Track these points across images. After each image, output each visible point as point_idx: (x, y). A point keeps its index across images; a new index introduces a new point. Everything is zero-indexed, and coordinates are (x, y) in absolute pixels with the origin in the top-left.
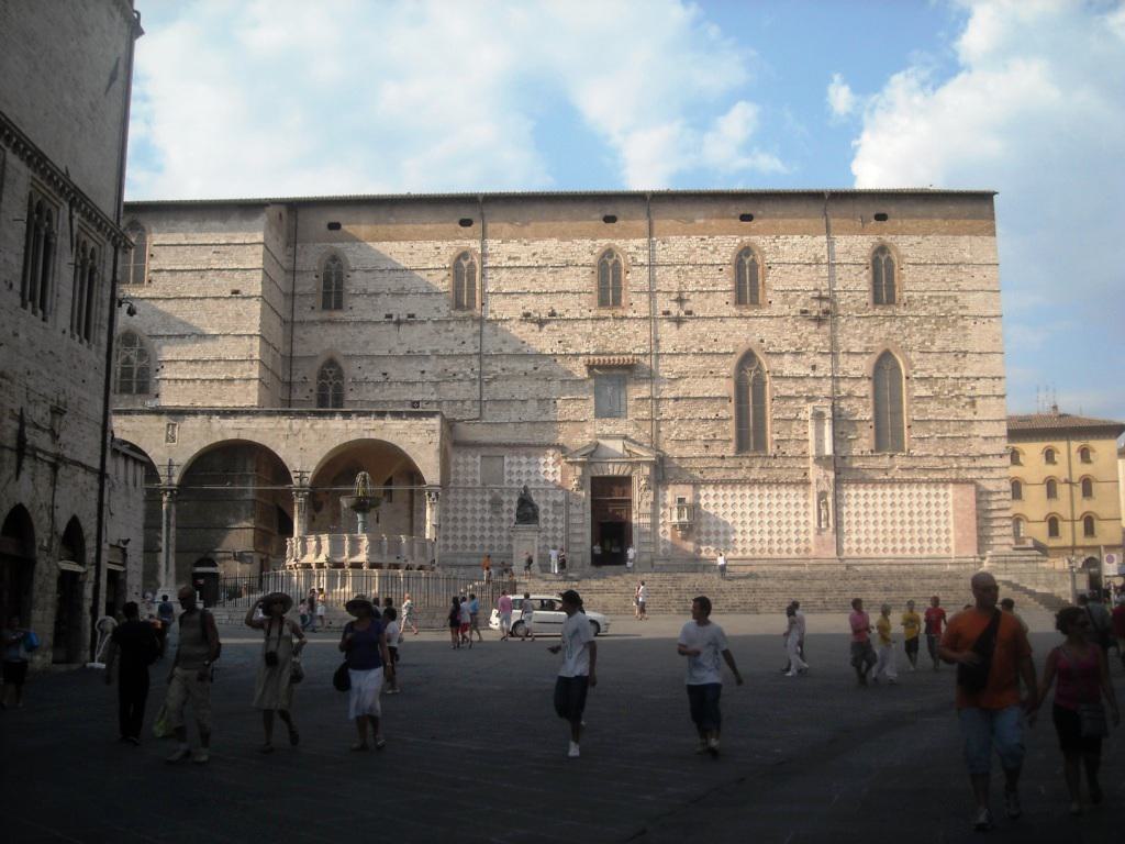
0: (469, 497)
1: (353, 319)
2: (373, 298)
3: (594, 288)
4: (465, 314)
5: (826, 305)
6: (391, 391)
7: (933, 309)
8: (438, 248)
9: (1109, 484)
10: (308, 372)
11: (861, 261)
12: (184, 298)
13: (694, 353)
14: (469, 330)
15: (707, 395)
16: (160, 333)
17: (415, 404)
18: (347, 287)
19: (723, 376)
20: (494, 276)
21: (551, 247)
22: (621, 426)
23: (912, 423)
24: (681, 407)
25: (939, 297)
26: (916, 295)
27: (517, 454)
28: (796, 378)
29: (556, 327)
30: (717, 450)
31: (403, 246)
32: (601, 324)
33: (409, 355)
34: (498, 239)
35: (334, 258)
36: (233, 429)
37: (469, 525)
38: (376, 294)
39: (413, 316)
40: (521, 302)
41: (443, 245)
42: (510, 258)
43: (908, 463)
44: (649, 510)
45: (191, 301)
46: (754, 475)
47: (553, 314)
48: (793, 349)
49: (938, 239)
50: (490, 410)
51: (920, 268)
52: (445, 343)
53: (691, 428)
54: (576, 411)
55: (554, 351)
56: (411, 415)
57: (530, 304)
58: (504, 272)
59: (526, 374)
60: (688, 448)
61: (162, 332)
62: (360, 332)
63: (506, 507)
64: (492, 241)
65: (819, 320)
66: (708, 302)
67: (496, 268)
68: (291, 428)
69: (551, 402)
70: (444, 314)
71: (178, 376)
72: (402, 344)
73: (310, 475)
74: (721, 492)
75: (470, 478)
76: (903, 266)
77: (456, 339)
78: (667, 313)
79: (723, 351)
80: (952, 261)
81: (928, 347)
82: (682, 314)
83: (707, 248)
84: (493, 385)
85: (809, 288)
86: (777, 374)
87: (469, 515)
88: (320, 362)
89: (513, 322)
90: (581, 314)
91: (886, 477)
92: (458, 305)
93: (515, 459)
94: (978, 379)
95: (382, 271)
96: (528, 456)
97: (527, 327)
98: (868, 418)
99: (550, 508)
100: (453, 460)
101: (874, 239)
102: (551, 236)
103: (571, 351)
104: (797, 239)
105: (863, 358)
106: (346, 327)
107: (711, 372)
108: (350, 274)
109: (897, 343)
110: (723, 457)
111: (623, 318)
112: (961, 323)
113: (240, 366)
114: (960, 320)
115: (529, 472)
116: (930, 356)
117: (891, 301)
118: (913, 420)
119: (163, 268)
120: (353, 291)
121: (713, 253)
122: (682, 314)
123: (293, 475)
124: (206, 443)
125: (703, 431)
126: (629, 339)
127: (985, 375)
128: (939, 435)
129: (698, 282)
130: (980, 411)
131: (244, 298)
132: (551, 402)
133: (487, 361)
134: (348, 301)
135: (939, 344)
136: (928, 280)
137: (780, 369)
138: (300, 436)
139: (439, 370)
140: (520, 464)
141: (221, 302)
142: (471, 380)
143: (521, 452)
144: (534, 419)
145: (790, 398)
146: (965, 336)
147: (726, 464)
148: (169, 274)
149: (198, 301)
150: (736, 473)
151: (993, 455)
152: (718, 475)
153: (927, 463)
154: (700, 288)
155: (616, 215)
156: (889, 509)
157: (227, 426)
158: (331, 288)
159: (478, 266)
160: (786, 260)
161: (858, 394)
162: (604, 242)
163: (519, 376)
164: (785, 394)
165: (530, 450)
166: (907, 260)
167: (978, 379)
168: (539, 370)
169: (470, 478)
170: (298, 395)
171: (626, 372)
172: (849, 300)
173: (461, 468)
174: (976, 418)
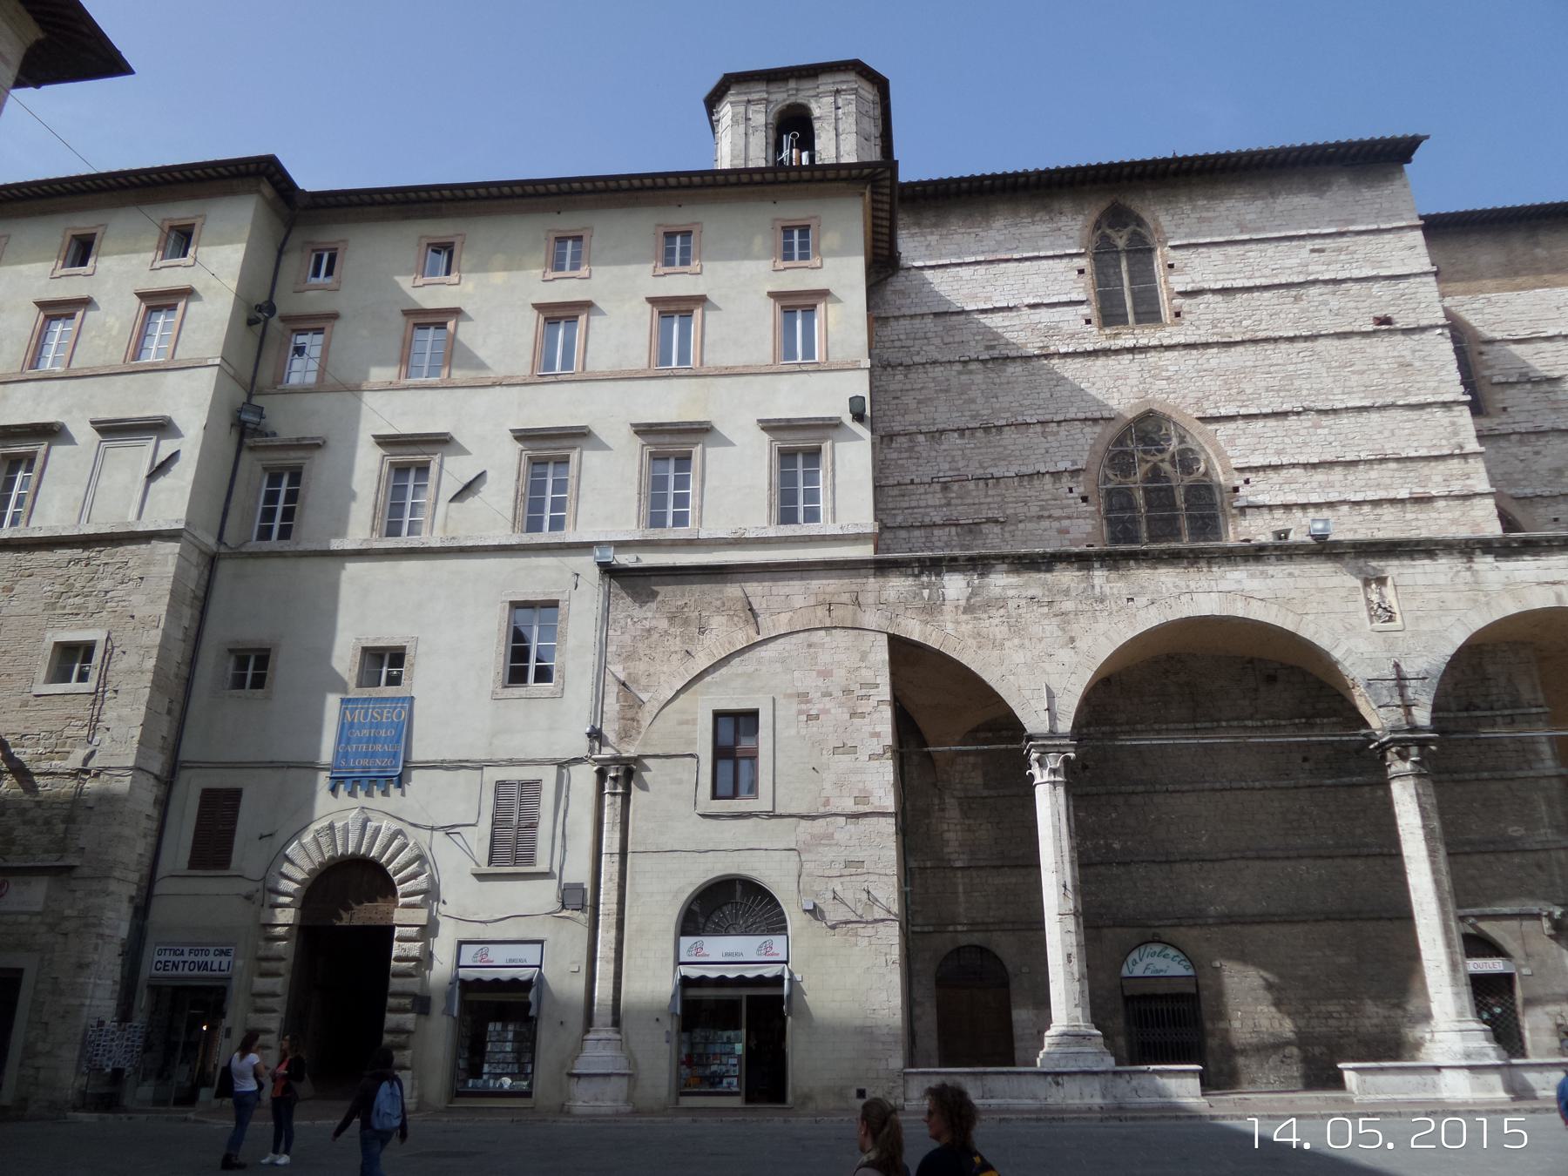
2: (1545, 387)
12: (1267, 340)
16: (1223, 412)
18: (1487, 373)
36: (1539, 584)
45: (1284, 346)
61: (1230, 410)
62: (1537, 453)
71: (1291, 498)
106: (1503, 443)
108: (1484, 348)
113: (1441, 466)
119: (1206, 286)
124: (1479, 620)
131: (1407, 332)
141: (1355, 342)
148: (1219, 298)
149: (1301, 345)
157: (1519, 576)
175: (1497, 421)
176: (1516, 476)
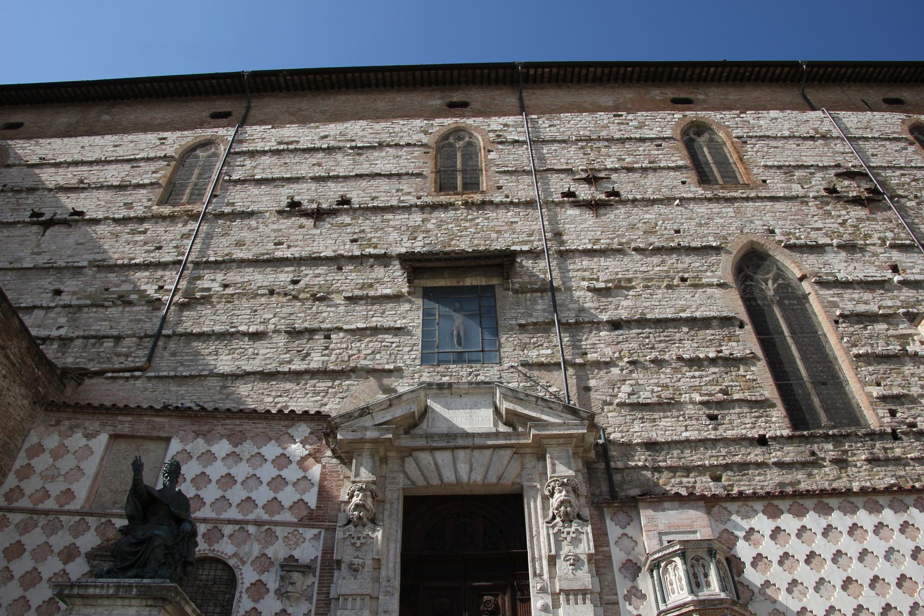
3: (428, 170)
19: (710, 285)
20: (248, 162)
24: (631, 340)
27: (205, 435)
44: (585, 578)
47: (344, 201)
50: (174, 354)
53: (664, 379)
57: (306, 194)
69: (319, 337)
72: (39, 254)
78: (570, 194)
83: (628, 124)
89: (267, 214)
90: (402, 201)
93: (200, 445)
96: (236, 439)
99: (272, 580)
100: (33, 439)
107: (683, 280)
110: (762, 441)
115: (228, 480)
121: (636, 128)
126: (499, 232)
140: (208, 457)
143: (220, 429)
144: (272, 367)
155: (467, 100)
162: (449, 122)
163: (255, 296)
165: (248, 426)
168: (302, 284)
171: (495, 281)
173: (42, 463)
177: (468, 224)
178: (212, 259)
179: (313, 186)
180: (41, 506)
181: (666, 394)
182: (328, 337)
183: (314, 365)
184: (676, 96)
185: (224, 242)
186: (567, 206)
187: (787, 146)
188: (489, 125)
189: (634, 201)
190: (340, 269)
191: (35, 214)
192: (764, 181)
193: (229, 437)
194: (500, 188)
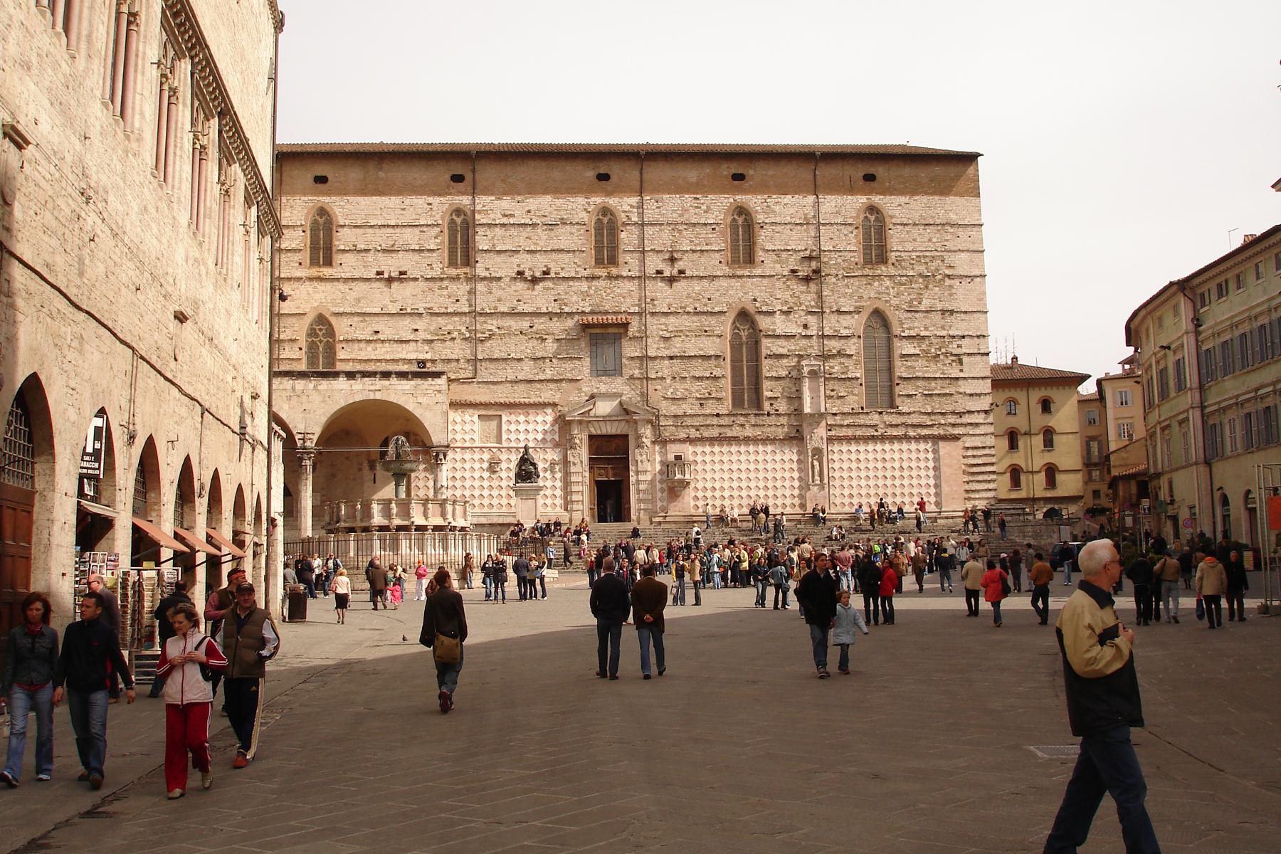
0: (468, 456)
1: (343, 275)
4: (458, 271)
5: (814, 265)
6: (384, 350)
7: (922, 269)
8: (431, 204)
9: (1070, 436)
10: (297, 331)
11: (850, 221)
13: (688, 313)
14: (462, 289)
15: (701, 353)
17: (422, 363)
18: (337, 243)
21: (544, 204)
22: (617, 384)
23: (897, 381)
25: (925, 257)
26: (903, 254)
28: (788, 337)
29: (551, 285)
30: (710, 408)
31: (394, 201)
32: (595, 283)
33: (402, 314)
34: (492, 194)
35: (322, 212)
37: (468, 483)
38: (367, 251)
39: (401, 273)
40: (516, 259)
41: (436, 200)
42: (505, 216)
43: (899, 420)
46: (749, 432)
48: (785, 308)
49: (925, 199)
51: (907, 228)
52: (440, 299)
54: (573, 369)
55: (550, 309)
56: (416, 375)
58: (497, 229)
59: (521, 333)
60: (684, 406)
63: (504, 465)
64: (484, 197)
65: (807, 280)
66: (702, 260)
67: (489, 225)
68: (293, 389)
70: (437, 272)
73: (315, 438)
74: (717, 449)
75: (467, 437)
76: (891, 226)
77: (450, 297)
78: (659, 272)
79: (716, 309)
80: (938, 222)
81: (916, 306)
82: (675, 272)
84: (488, 344)
85: (800, 248)
86: (770, 333)
87: (467, 475)
88: (308, 320)
90: (577, 273)
91: (876, 434)
92: (452, 263)
93: (513, 418)
94: (963, 337)
95: (371, 226)
97: (520, 285)
98: (858, 375)
101: (863, 199)
102: (544, 193)
103: (567, 309)
104: (788, 199)
105: (853, 317)
107: (706, 331)
109: (886, 301)
110: (718, 415)
111: (618, 277)
112: (948, 282)
114: (947, 279)
116: (917, 315)
117: (883, 259)
118: (901, 378)
120: (342, 247)
121: (705, 212)
122: (675, 272)
123: (297, 437)
125: (699, 389)
127: (971, 334)
128: (926, 392)
129: (691, 241)
130: (965, 367)
132: (548, 361)
133: (482, 319)
134: (338, 258)
135: (925, 305)
136: (915, 240)
137: (772, 327)
138: (304, 398)
139: (432, 328)
142: (466, 339)
144: (531, 377)
145: (781, 356)
146: (951, 295)
147: (722, 422)
150: (732, 430)
151: (978, 412)
152: (714, 432)
153: (914, 419)
154: (694, 248)
155: (609, 173)
156: (880, 465)
158: (319, 244)
159: (471, 224)
160: (778, 220)
161: (848, 353)
162: (598, 200)
164: (777, 353)
166: (894, 221)
167: (963, 337)
169: (467, 437)
170: (288, 352)
171: (622, 330)
172: (839, 260)
174: (962, 375)
175: (335, 270)
176: (337, 301)
177: (609, 291)
178: (489, 312)
179: (528, 256)
180: (465, 445)
181: (686, 393)
182: (551, 361)
183: (549, 377)
184: (736, 172)
185: (491, 298)
186: (659, 280)
187: (785, 231)
188: (622, 206)
189: (692, 277)
190: (551, 319)
191: (378, 273)
192: (763, 262)
193: (523, 414)
194: (626, 263)
